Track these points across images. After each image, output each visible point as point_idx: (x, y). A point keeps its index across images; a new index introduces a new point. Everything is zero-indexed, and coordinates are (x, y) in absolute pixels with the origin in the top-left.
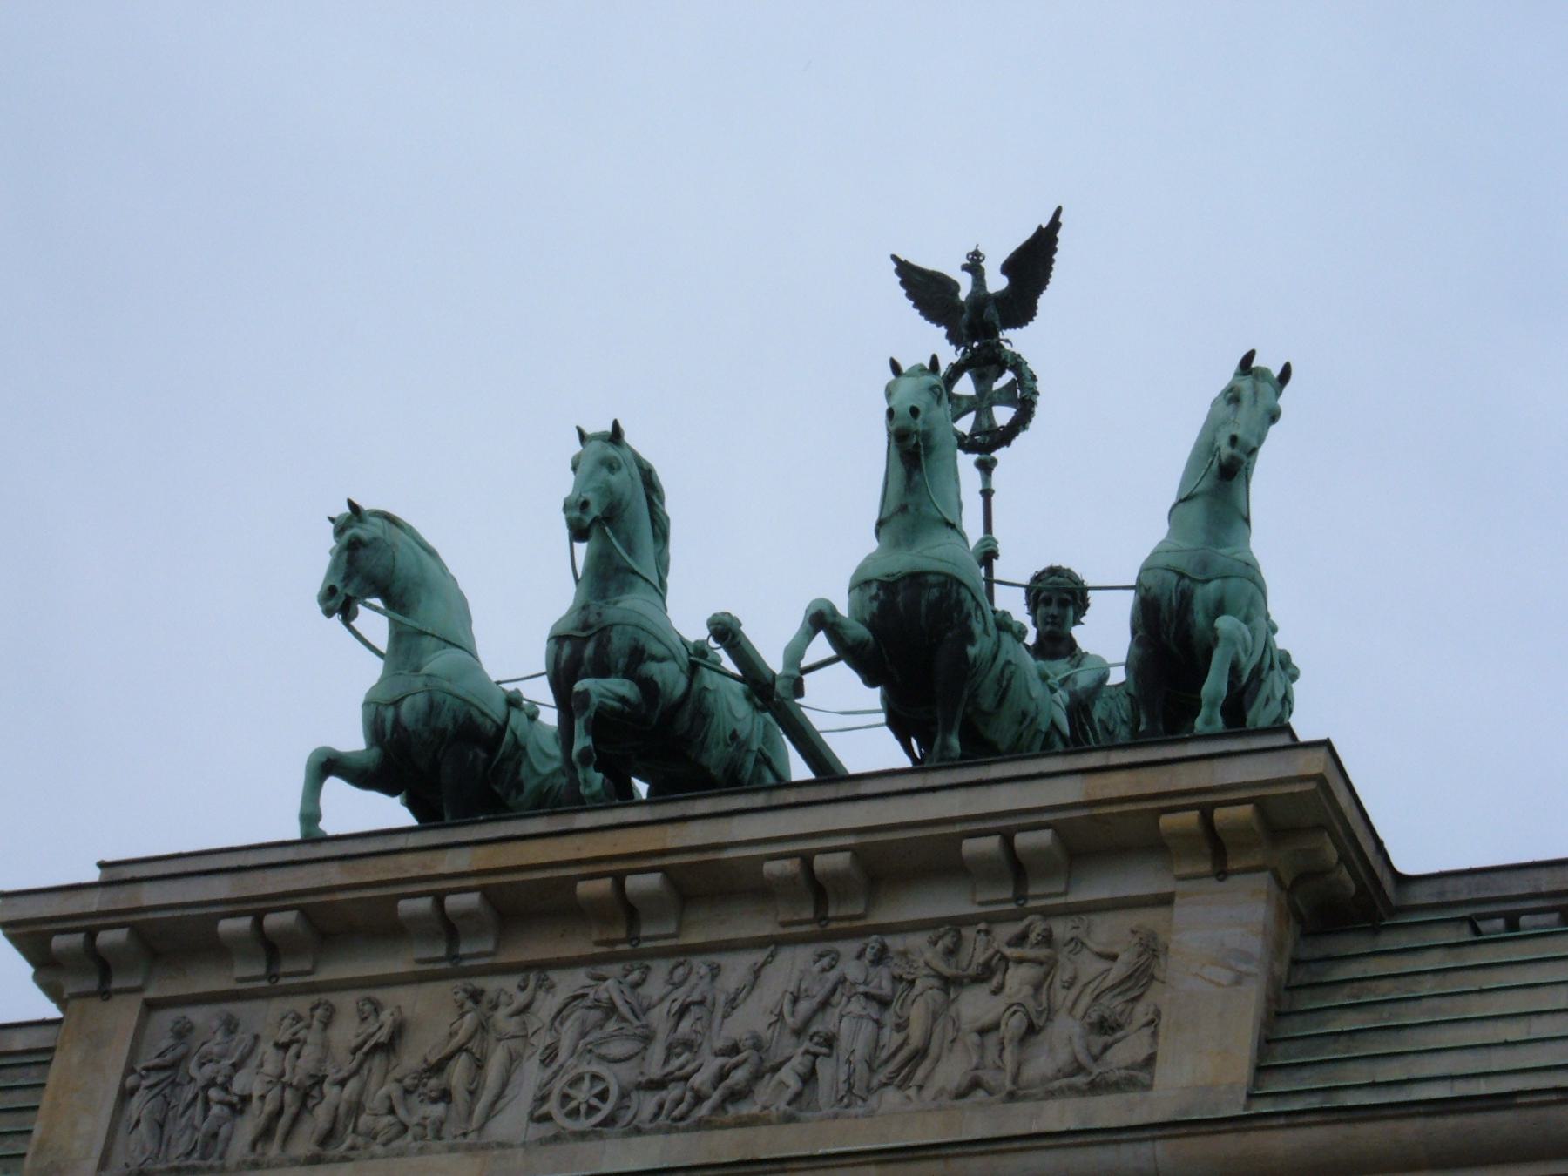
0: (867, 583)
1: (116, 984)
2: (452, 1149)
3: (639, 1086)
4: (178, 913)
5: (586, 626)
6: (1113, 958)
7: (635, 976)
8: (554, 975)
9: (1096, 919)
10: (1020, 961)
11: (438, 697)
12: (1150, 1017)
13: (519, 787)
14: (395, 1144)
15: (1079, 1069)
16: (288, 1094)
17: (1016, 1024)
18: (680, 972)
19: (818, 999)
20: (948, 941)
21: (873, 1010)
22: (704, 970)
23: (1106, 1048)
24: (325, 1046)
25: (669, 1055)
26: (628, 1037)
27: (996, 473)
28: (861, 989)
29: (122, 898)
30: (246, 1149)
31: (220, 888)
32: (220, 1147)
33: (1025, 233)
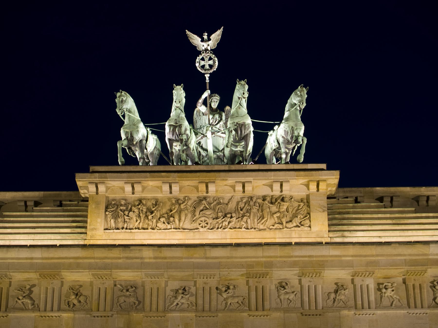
5: (176, 123)
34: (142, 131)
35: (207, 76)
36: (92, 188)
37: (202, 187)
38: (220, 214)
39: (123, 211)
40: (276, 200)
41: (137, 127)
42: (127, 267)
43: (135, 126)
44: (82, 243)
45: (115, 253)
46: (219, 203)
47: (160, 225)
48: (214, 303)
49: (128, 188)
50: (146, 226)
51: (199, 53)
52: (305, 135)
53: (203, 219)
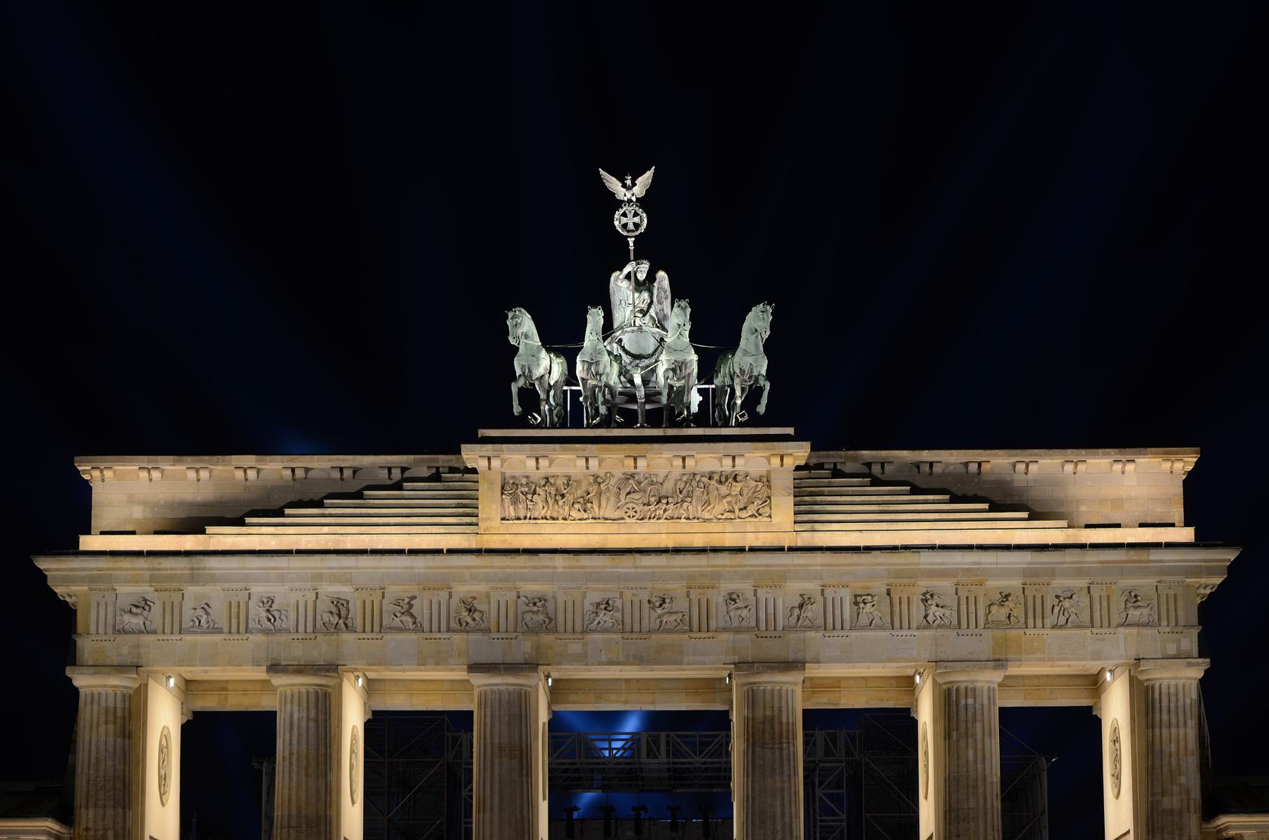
34: (545, 358)
35: (631, 241)
36: (484, 463)
37: (631, 462)
38: (652, 499)
39: (525, 494)
40: (727, 479)
41: (538, 359)
42: (535, 580)
43: (535, 356)
44: (471, 543)
45: (522, 560)
46: (652, 483)
47: (574, 514)
48: (645, 622)
49: (532, 463)
50: (555, 515)
51: (619, 204)
52: (769, 376)
53: (630, 505)
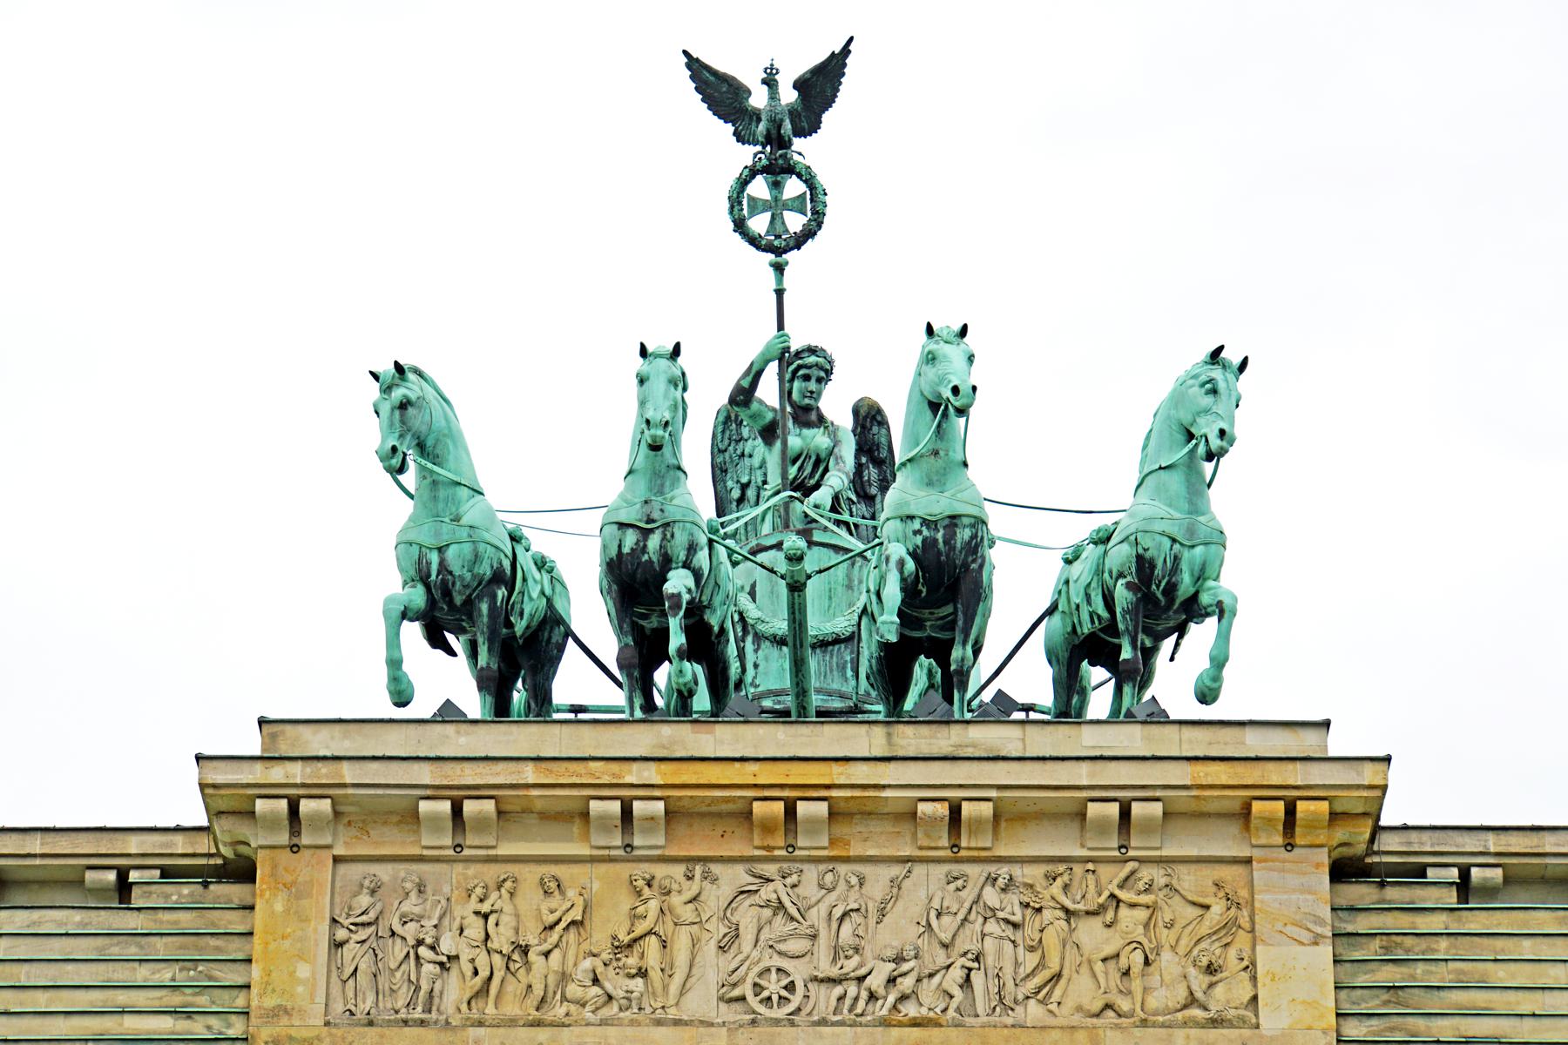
0: (912, 518)
1: (305, 840)
2: (659, 1023)
3: (815, 979)
4: (380, 792)
6: (1207, 907)
7: (794, 879)
8: (716, 869)
9: (1182, 869)
10: (1133, 906)
11: (482, 547)
12: (1246, 963)
13: (521, 614)
14: (606, 1012)
15: (1192, 1001)
16: (497, 959)
17: (1138, 957)
18: (829, 877)
19: (961, 916)
20: (1066, 878)
21: (1009, 931)
22: (854, 880)
23: (1211, 985)
24: (517, 916)
25: (837, 953)
26: (801, 936)
27: (787, 269)
28: (1001, 915)
29: (324, 773)
30: (464, 1007)
31: (424, 774)
32: (436, 1001)
33: (820, 56)
